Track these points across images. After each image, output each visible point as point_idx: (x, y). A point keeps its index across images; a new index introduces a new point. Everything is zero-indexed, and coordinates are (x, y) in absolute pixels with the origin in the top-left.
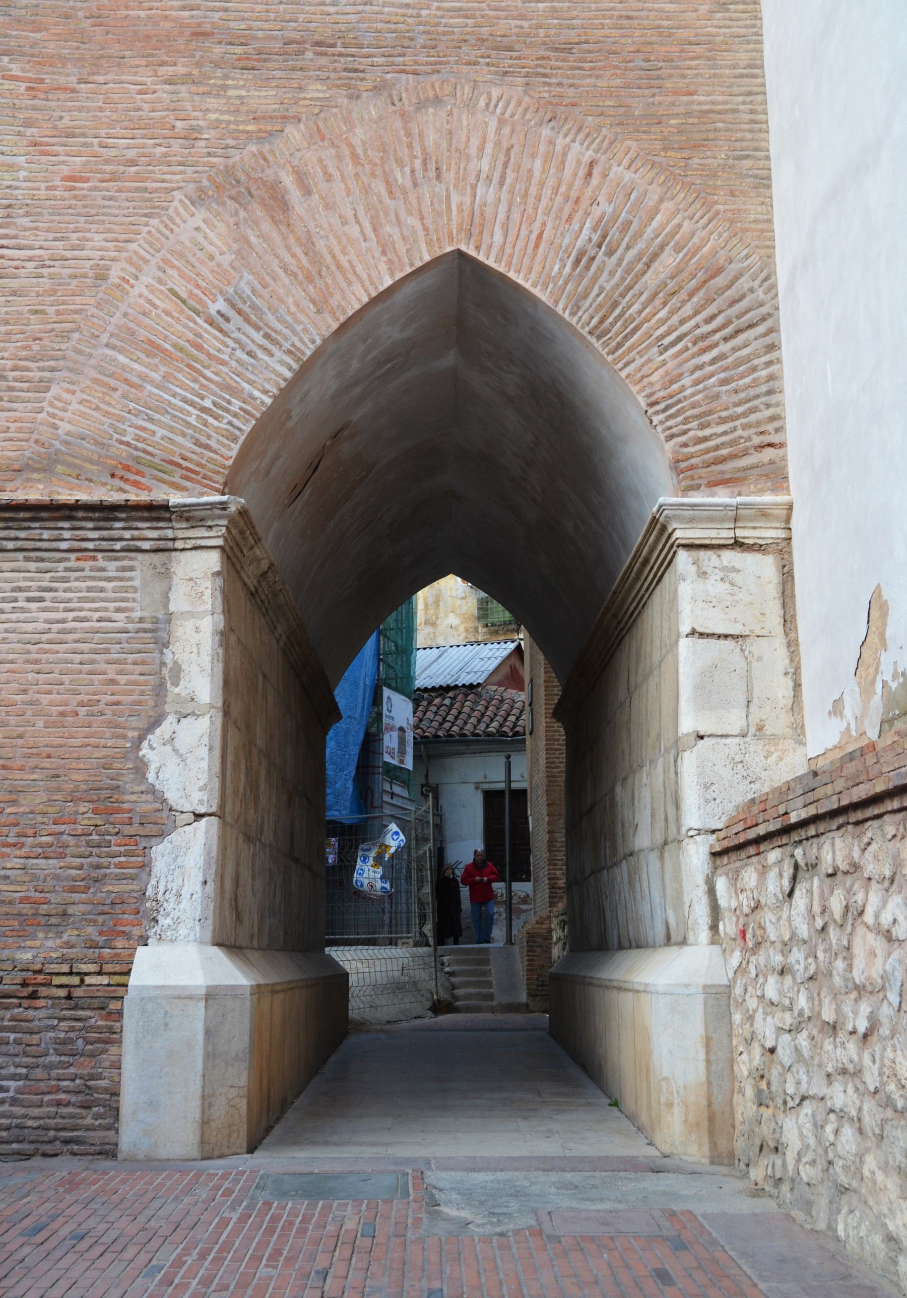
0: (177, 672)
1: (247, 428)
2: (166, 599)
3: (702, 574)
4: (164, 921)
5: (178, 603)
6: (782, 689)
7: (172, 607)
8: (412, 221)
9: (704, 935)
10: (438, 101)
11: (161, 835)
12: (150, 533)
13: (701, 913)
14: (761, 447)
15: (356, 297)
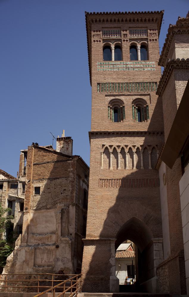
0: (112, 254)
1: (117, 233)
2: (110, 247)
3: (156, 245)
4: (112, 274)
5: (112, 248)
6: (162, 255)
7: (111, 248)
8: (130, 214)
9: (156, 275)
10: (132, 203)
11: (111, 268)
12: (109, 242)
13: (155, 273)
14: (160, 234)
15: (126, 221)
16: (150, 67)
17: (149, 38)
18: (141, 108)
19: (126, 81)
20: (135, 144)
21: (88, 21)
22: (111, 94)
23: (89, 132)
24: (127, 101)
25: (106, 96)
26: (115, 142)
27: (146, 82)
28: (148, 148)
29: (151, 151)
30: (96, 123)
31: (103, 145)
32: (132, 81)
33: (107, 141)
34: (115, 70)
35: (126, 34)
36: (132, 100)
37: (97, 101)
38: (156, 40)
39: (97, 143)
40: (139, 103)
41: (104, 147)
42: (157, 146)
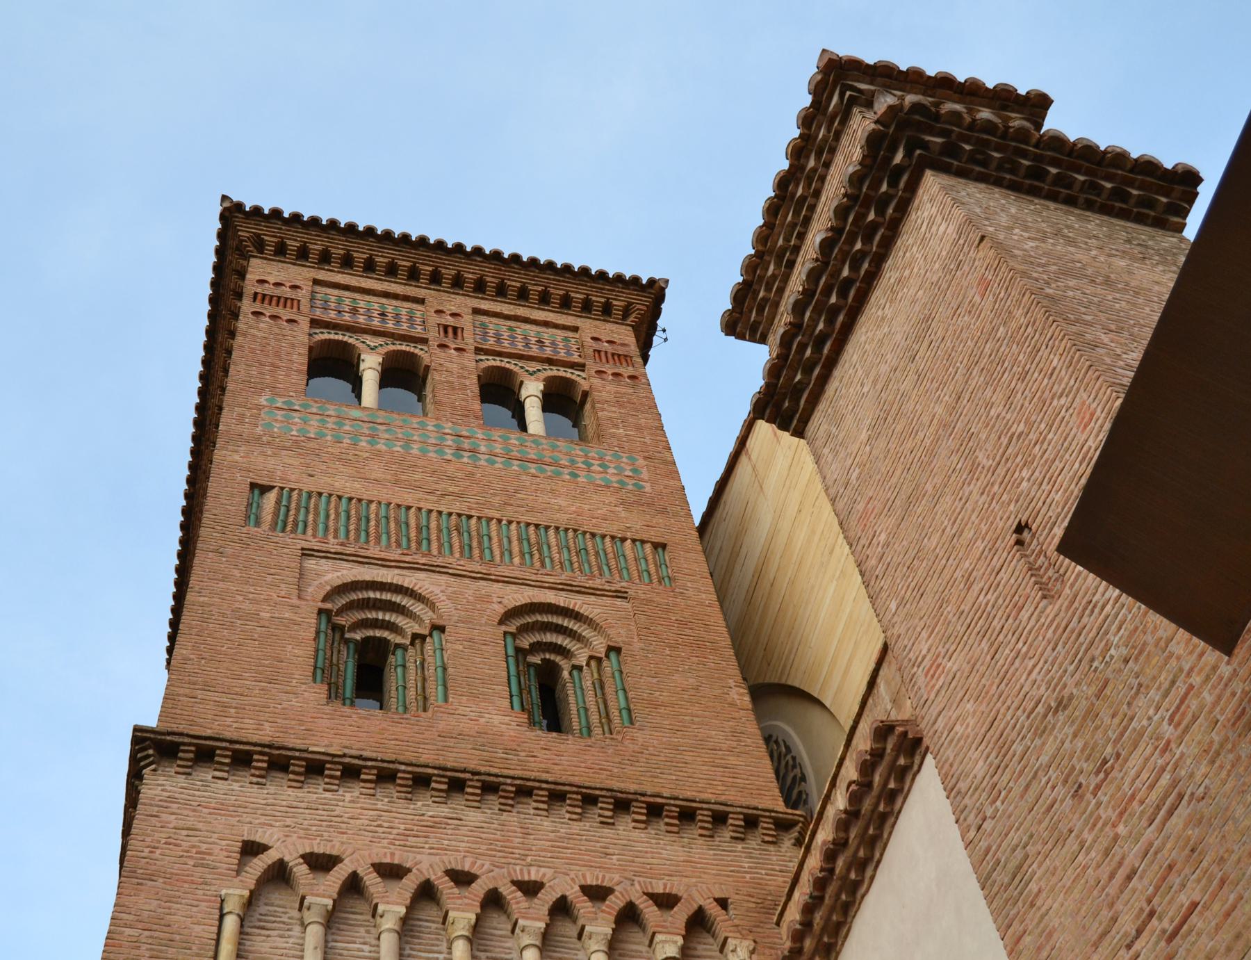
16: (611, 471)
17: (592, 366)
18: (565, 674)
19: (457, 507)
20: (534, 875)
21: (232, 243)
22: (350, 550)
23: (137, 729)
24: (463, 611)
25: (306, 553)
26: (360, 826)
27: (593, 535)
28: (650, 912)
29: (680, 941)
30: (206, 687)
31: (251, 849)
32: (497, 515)
33: (289, 821)
34: (381, 447)
35: (455, 329)
36: (501, 610)
37: (236, 573)
38: (632, 377)
39: (200, 826)
40: (550, 638)
41: (259, 865)
42: (723, 903)
